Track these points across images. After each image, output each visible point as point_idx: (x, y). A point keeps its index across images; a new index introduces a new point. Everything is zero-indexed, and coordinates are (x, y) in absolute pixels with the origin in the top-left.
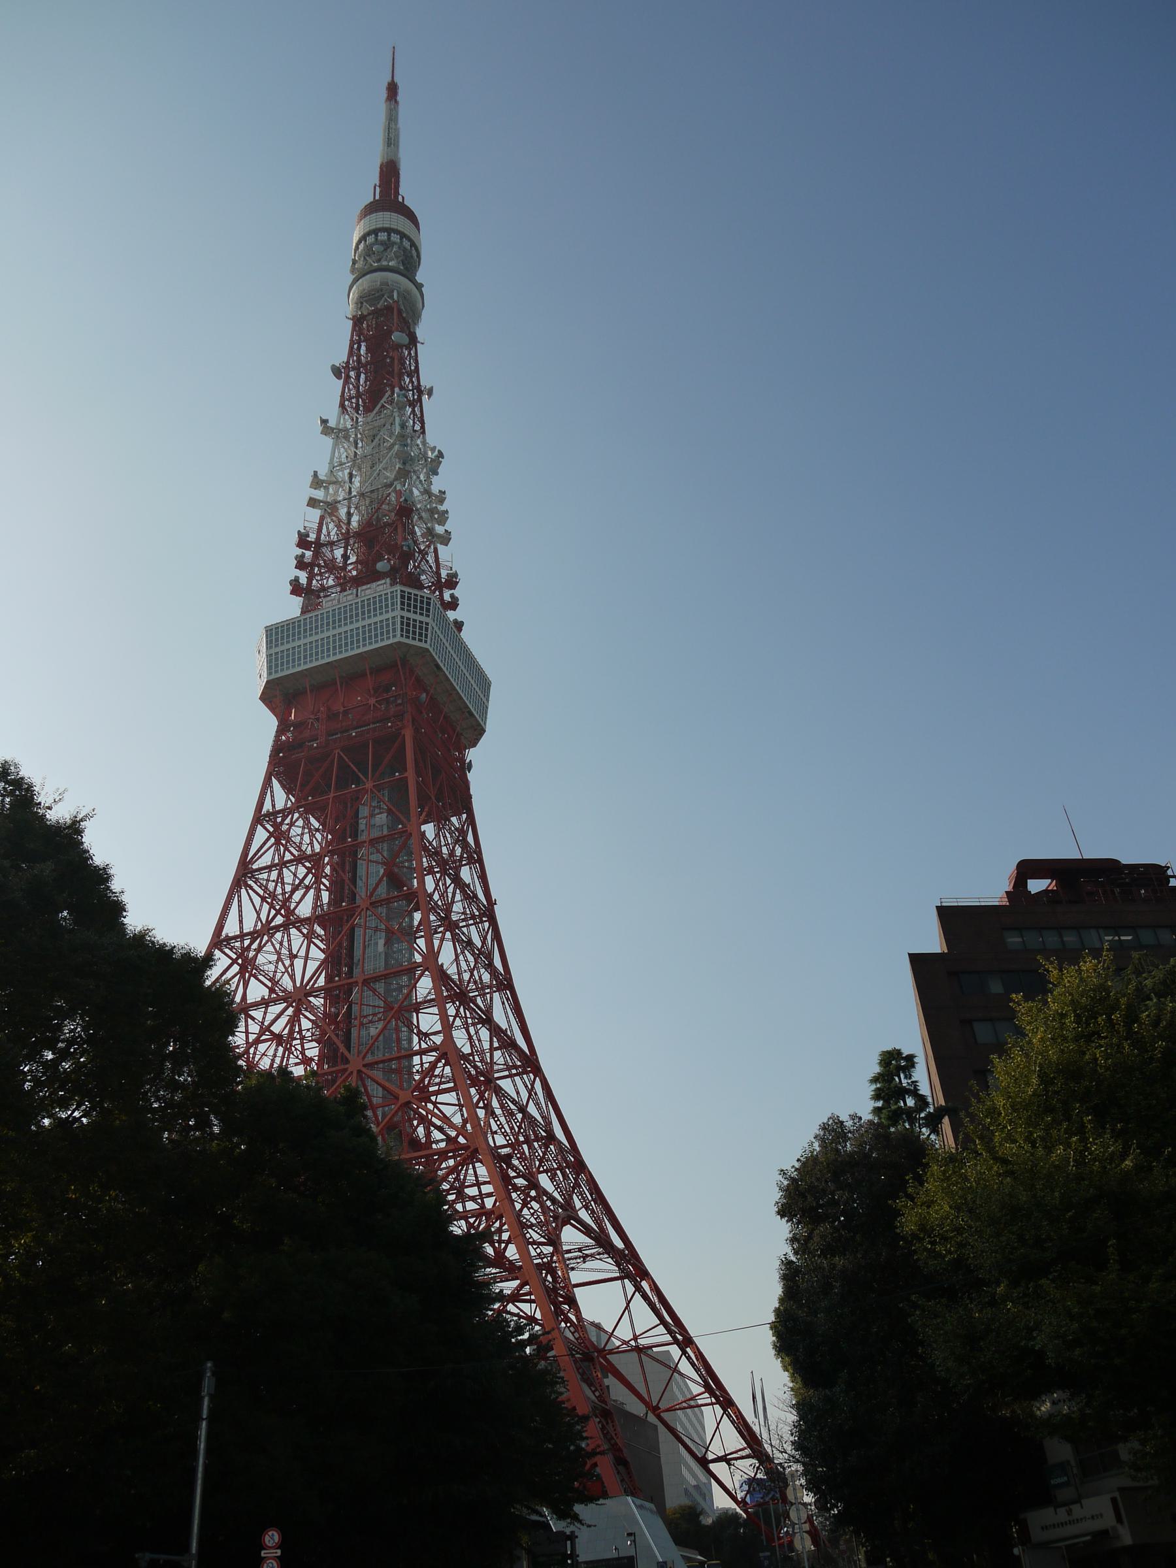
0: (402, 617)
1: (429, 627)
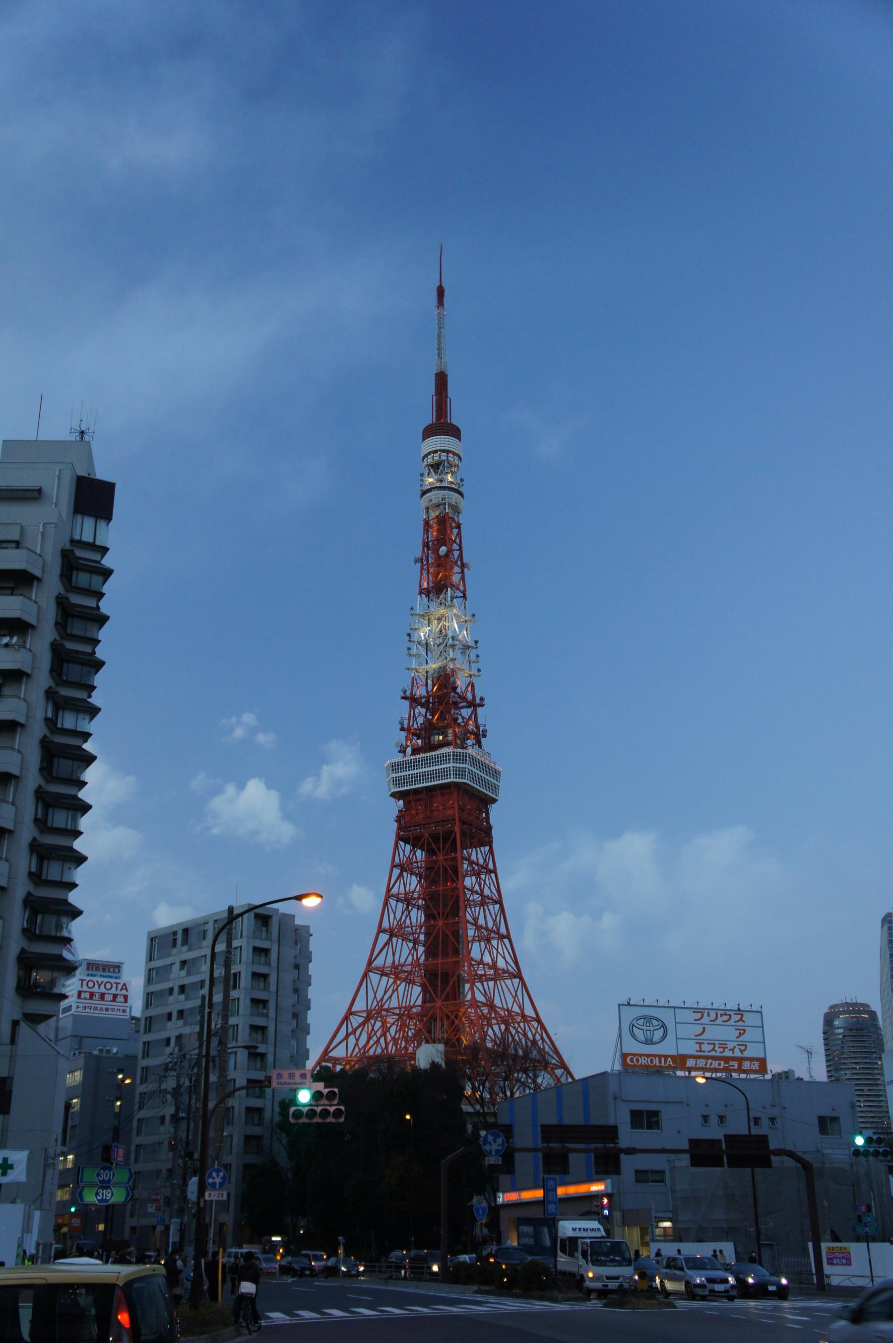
0: (454, 767)
1: (467, 770)
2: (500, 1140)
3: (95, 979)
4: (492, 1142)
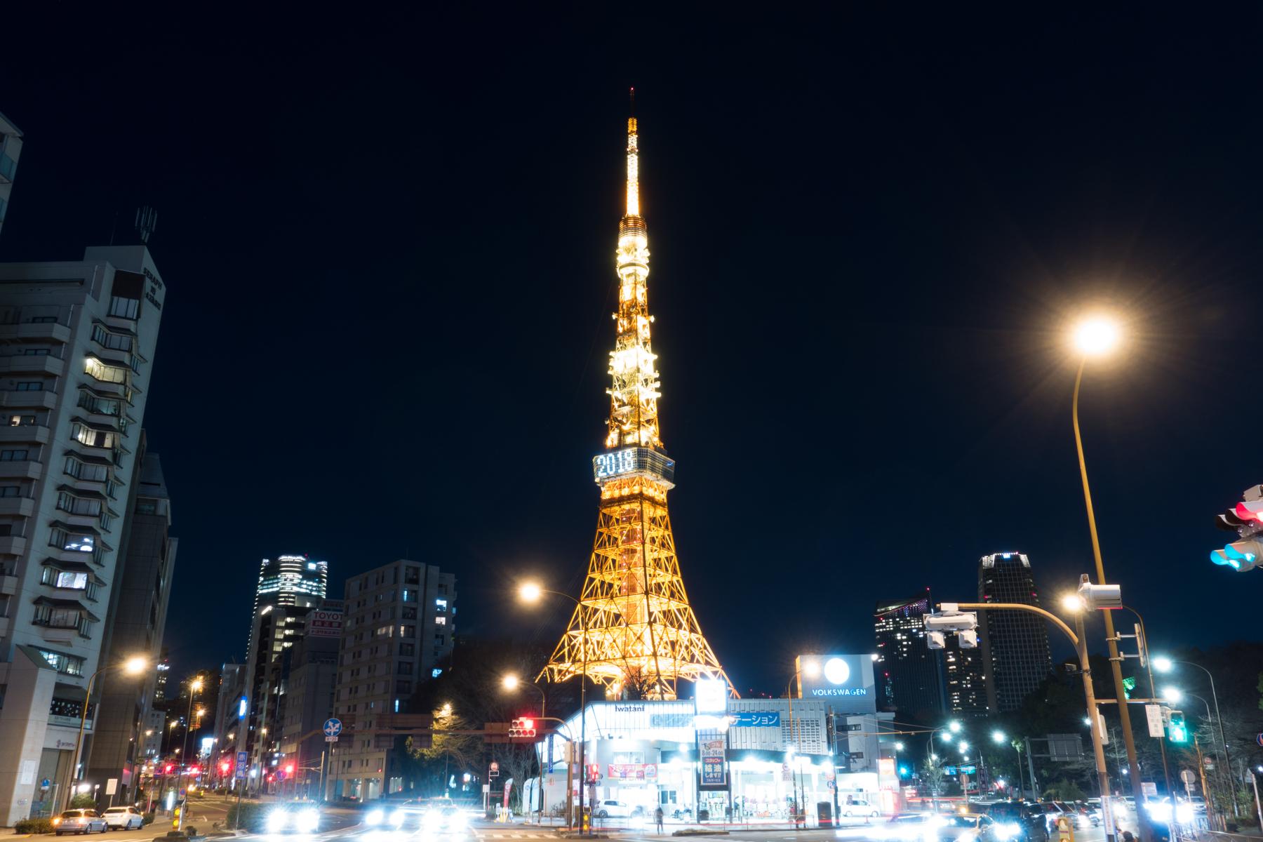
2: (337, 725)
3: (329, 613)
4: (332, 727)
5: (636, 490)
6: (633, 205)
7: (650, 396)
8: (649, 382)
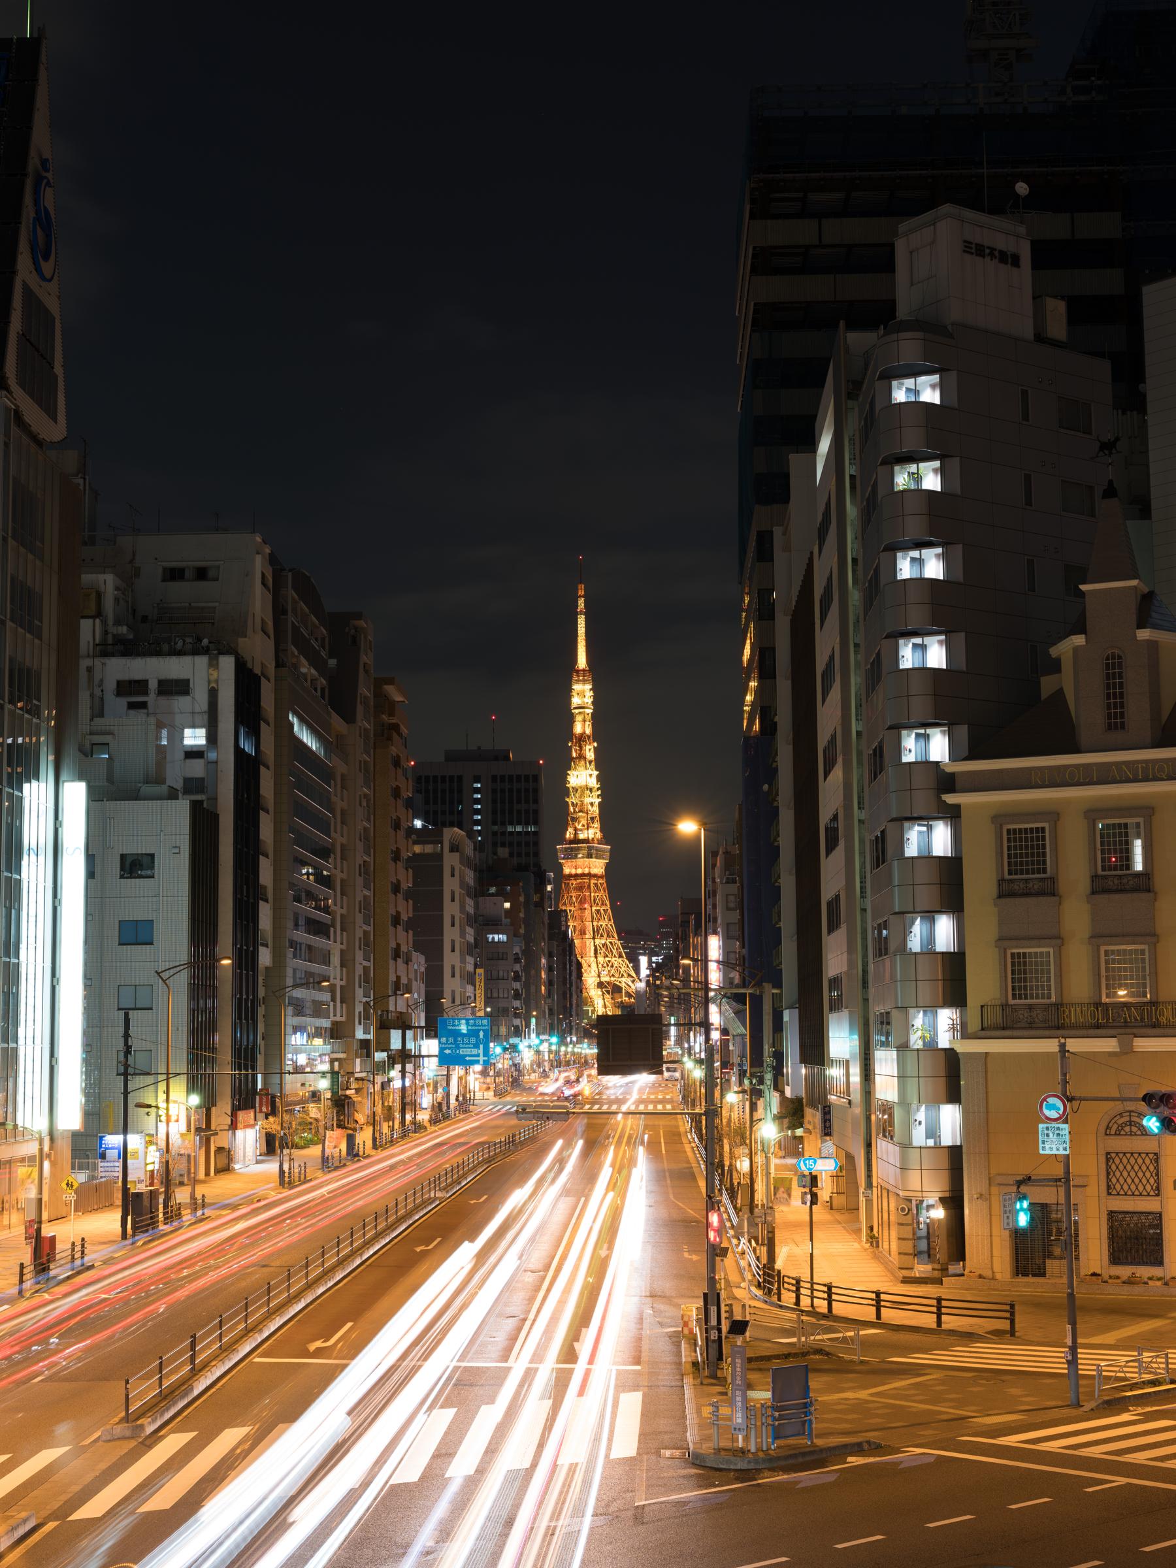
5: (586, 871)
6: (582, 661)
7: (593, 801)
8: (593, 790)
